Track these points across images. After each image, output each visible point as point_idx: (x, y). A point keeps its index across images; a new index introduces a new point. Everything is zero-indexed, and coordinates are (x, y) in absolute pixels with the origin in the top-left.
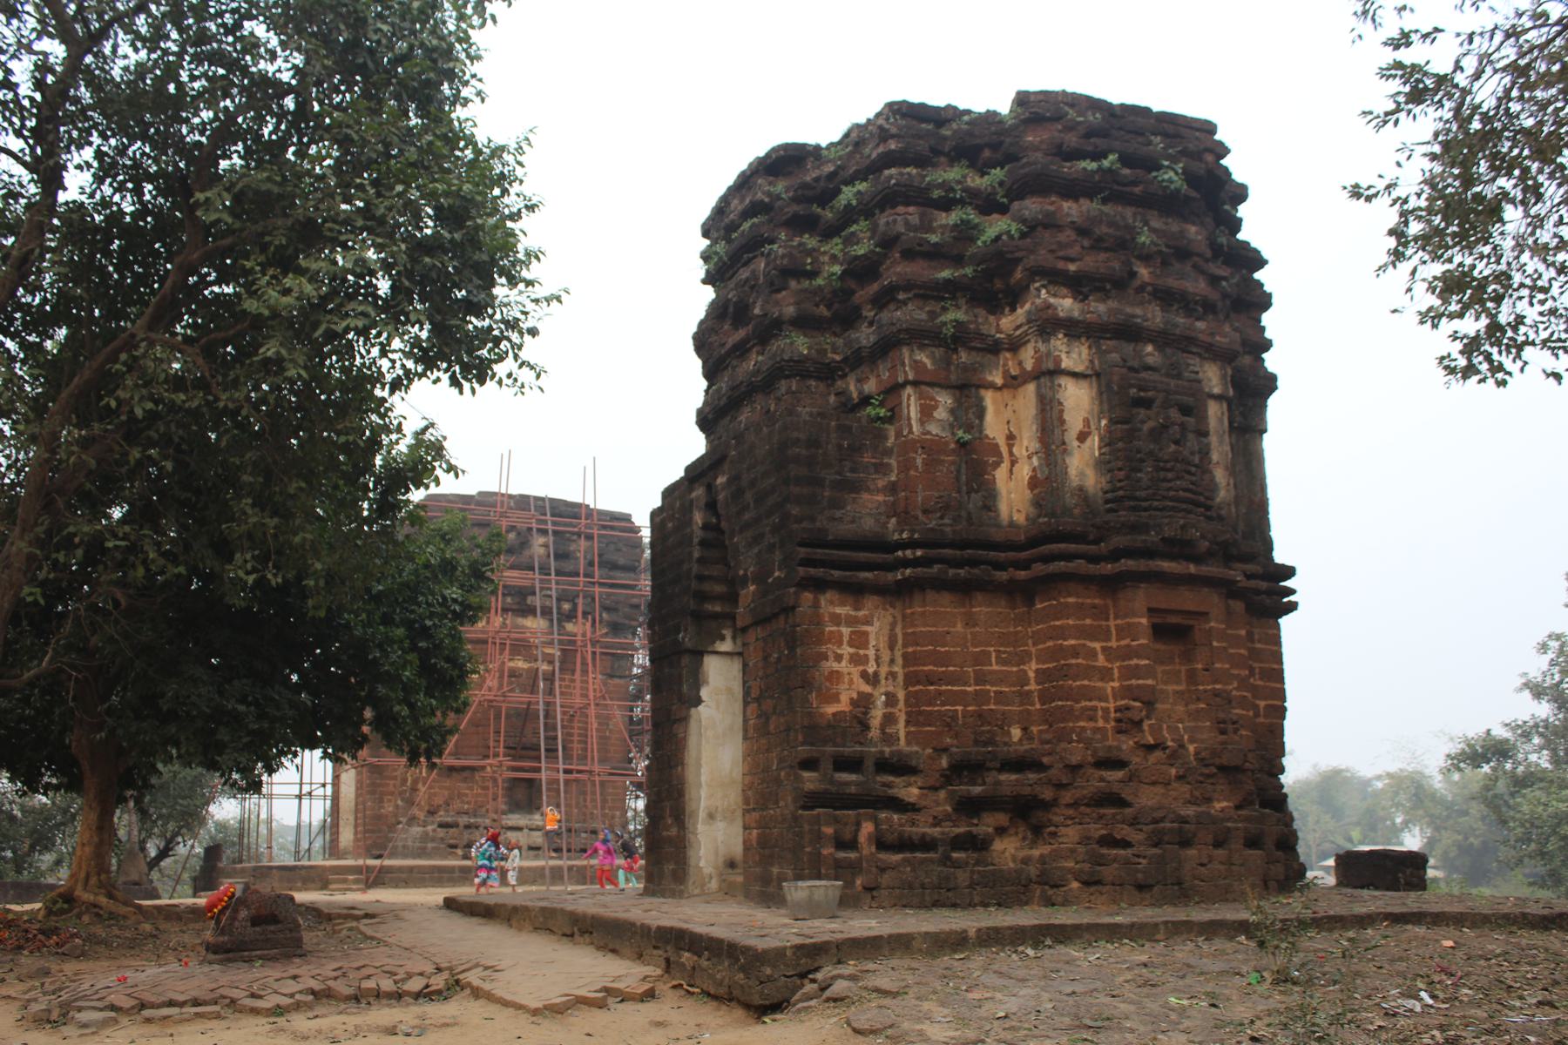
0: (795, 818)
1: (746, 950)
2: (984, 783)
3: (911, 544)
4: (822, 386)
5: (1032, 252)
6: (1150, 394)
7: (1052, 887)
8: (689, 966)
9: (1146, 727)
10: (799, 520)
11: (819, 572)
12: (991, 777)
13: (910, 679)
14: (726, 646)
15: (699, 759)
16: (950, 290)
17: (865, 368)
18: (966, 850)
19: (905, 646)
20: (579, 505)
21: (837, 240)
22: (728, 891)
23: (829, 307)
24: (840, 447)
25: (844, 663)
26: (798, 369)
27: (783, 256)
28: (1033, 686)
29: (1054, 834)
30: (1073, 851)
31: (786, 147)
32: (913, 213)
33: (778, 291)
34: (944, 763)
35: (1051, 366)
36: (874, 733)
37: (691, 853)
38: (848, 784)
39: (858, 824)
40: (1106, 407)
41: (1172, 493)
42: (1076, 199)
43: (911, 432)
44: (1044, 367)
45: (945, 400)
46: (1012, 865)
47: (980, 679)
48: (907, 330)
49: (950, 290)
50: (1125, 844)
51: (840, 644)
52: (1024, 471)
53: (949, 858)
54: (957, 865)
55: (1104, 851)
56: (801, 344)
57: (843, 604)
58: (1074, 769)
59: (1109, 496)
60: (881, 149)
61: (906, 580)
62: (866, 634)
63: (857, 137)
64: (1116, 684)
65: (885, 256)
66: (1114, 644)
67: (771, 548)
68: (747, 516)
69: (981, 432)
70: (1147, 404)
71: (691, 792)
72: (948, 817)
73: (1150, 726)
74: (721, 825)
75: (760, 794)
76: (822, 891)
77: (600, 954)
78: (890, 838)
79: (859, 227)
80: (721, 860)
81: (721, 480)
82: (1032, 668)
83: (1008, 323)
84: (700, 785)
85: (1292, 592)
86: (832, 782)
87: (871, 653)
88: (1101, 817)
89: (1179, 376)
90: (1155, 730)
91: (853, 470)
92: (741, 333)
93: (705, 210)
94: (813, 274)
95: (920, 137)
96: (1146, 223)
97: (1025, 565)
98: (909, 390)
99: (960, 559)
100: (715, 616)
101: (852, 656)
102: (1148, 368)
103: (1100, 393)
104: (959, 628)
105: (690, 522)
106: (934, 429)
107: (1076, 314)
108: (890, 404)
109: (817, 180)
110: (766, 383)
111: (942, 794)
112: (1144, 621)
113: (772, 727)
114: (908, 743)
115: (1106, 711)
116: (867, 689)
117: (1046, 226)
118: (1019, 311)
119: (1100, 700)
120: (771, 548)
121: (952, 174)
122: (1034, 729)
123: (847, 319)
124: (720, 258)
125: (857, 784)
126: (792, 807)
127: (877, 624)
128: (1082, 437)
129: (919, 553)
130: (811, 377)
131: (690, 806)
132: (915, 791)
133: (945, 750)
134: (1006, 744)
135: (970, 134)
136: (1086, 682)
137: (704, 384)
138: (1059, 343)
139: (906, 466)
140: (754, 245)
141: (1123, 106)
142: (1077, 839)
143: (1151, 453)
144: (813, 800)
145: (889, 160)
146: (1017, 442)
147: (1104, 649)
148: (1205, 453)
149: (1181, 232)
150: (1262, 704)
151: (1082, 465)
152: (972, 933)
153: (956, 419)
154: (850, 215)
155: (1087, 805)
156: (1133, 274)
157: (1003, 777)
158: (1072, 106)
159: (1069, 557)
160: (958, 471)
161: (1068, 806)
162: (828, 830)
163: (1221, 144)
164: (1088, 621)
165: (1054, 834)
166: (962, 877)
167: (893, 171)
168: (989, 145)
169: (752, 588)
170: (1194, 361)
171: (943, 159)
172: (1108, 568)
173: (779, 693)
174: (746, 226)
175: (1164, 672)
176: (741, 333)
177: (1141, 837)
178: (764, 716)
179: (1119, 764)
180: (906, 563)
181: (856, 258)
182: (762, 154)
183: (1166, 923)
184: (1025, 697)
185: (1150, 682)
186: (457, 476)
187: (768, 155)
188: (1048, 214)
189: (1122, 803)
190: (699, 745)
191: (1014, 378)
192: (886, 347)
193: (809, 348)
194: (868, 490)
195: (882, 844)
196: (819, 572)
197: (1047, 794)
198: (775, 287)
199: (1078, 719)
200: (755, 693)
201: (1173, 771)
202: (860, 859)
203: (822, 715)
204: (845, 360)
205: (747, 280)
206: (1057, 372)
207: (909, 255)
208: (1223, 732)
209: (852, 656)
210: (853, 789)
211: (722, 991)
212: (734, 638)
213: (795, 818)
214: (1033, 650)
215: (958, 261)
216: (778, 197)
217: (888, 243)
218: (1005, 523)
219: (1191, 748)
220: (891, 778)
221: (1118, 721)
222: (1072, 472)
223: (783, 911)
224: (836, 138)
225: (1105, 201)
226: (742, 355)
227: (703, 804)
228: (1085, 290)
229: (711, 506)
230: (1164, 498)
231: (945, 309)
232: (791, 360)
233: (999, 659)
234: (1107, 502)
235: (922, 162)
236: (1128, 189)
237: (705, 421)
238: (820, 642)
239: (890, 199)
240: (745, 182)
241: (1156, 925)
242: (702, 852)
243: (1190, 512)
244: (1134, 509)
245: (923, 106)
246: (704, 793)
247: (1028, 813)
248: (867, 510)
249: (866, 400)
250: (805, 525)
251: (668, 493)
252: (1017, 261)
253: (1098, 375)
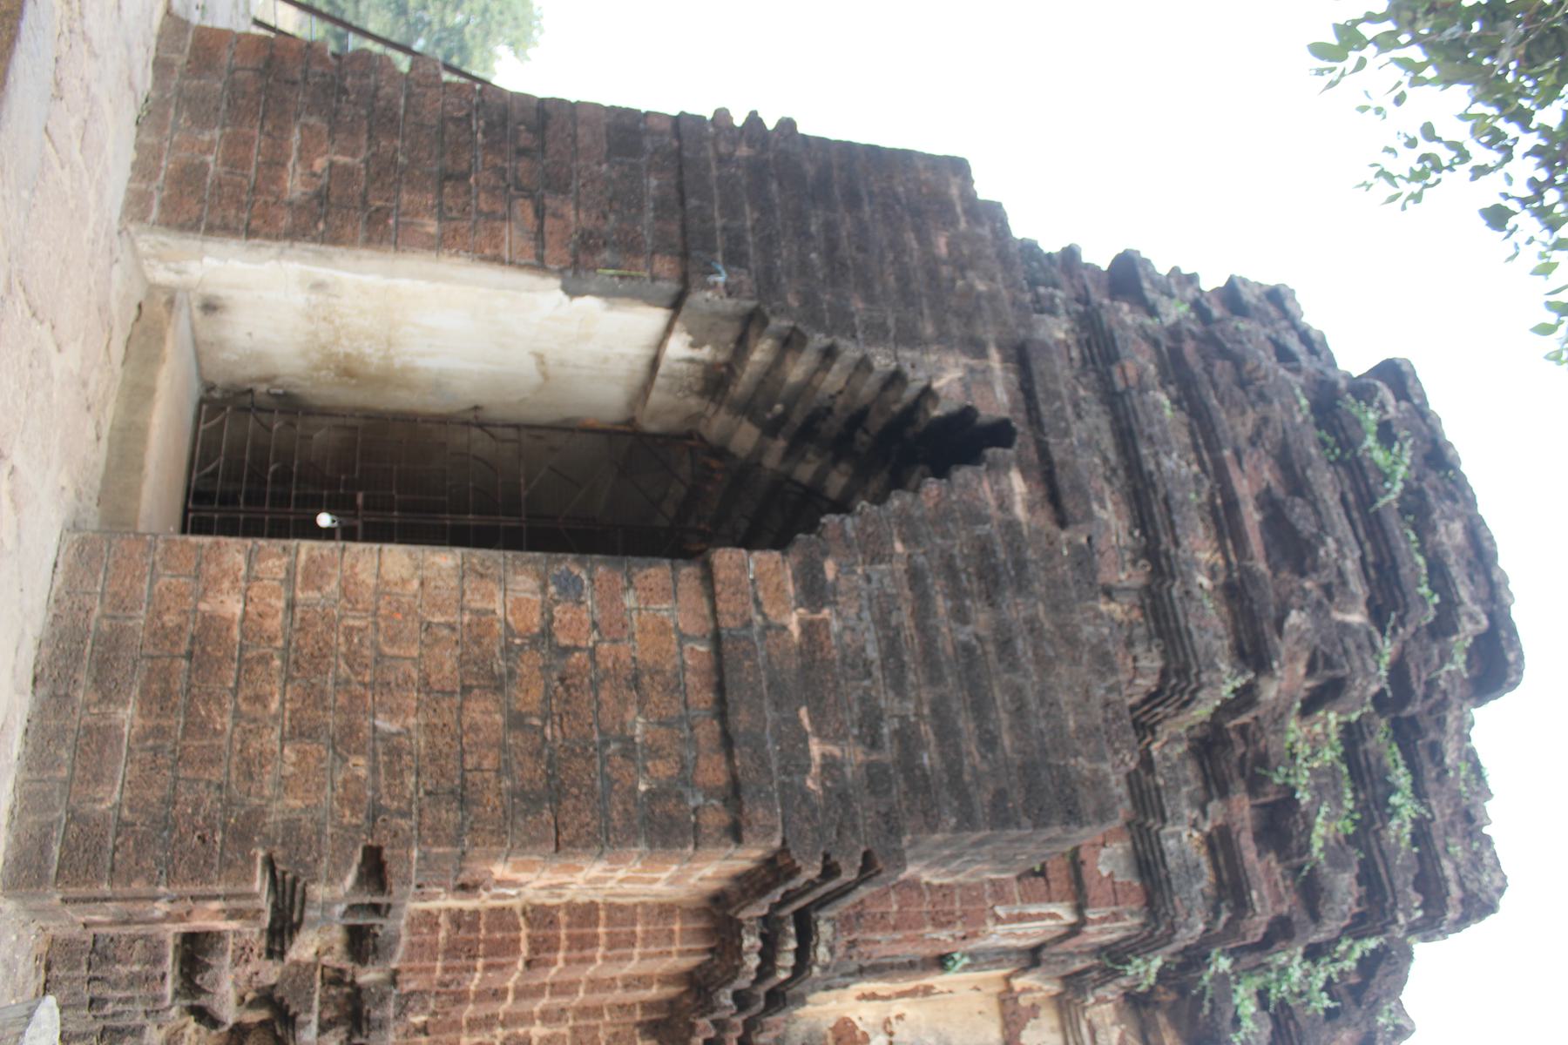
0: (242, 836)
14: (678, 347)
37: (234, 246)
43: (998, 920)
60: (1455, 891)
61: (738, 952)
74: (300, 298)
80: (222, 292)
100: (742, 344)
110: (1161, 616)
154: (1374, 809)
169: (793, 622)
186: (1319, 50)
212: (691, 361)
226: (1214, 510)
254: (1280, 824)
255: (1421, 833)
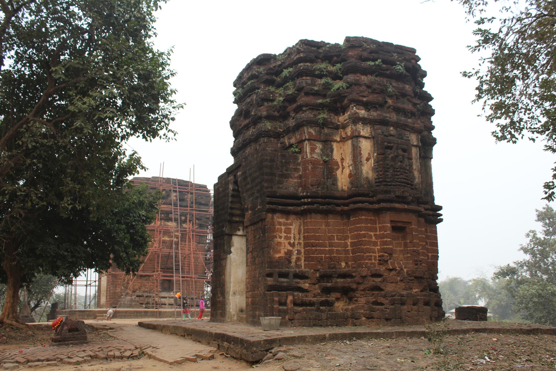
0: (265, 294)
1: (247, 341)
2: (332, 282)
3: (307, 197)
4: (275, 140)
5: (351, 94)
6: (392, 145)
7: (356, 319)
8: (226, 347)
9: (389, 263)
10: (267, 188)
11: (274, 207)
12: (334, 280)
13: (306, 245)
14: (240, 233)
15: (230, 273)
16: (321, 107)
17: (291, 134)
18: (325, 306)
19: (304, 233)
20: (188, 182)
21: (281, 88)
22: (240, 320)
23: (278, 112)
24: (282, 162)
25: (282, 239)
26: (267, 134)
27: (262, 94)
28: (349, 248)
29: (356, 301)
30: (363, 306)
31: (264, 55)
32: (309, 79)
33: (260, 106)
34: (318, 275)
35: (357, 134)
36: (293, 264)
37: (227, 307)
38: (283, 282)
39: (287, 297)
40: (376, 149)
41: (399, 180)
42: (366, 75)
43: (307, 157)
44: (354, 135)
45: (319, 146)
46: (341, 311)
47: (331, 245)
48: (306, 121)
49: (321, 107)
50: (382, 304)
51: (281, 232)
52: (347, 171)
53: (319, 309)
54: (322, 311)
55: (374, 306)
56: (268, 125)
57: (282, 218)
58: (364, 277)
59: (377, 180)
60: (297, 56)
61: (305, 210)
62: (290, 229)
63: (289, 52)
64: (379, 247)
65: (299, 94)
66: (378, 233)
67: (257, 198)
68: (248, 186)
69: (332, 157)
70: (390, 148)
71: (227, 285)
72: (319, 294)
73: (391, 262)
74: (238, 297)
75: (252, 285)
76: (274, 320)
77: (194, 343)
78: (298, 302)
79: (289, 84)
80: (238, 309)
81: (239, 173)
82: (349, 241)
83: (342, 119)
84: (230, 282)
85: (441, 215)
86: (278, 281)
87: (292, 235)
88: (373, 294)
89: (402, 138)
90: (392, 264)
91: (286, 170)
92: (247, 121)
93: (235, 78)
94: (273, 101)
95: (312, 52)
96: (391, 84)
97: (347, 205)
98: (306, 142)
99: (324, 202)
100: (237, 222)
101: (285, 236)
102: (391, 135)
103: (374, 144)
104: (324, 227)
105: (228, 188)
106: (315, 156)
107: (366, 116)
108: (300, 147)
109: (275, 67)
110: (256, 139)
111: (317, 286)
112: (389, 225)
113: (256, 262)
114: (305, 268)
115: (375, 257)
116: (291, 248)
117: (355, 85)
118: (346, 114)
119: (373, 253)
120: (257, 198)
121: (323, 66)
122: (350, 263)
123: (285, 117)
124: (240, 94)
125: (287, 282)
126: (263, 290)
127: (294, 225)
128: (368, 160)
129: (309, 200)
130: (271, 137)
131: (227, 290)
132: (307, 285)
133: (318, 270)
134: (339, 268)
135: (328, 51)
136: (368, 247)
137: (234, 139)
138: (360, 126)
139: (305, 169)
140: (252, 89)
141: (383, 42)
142: (364, 302)
143: (392, 166)
144: (271, 288)
145: (300, 60)
146: (345, 161)
147: (375, 235)
148: (411, 165)
149: (403, 87)
150: (430, 255)
151: (367, 169)
152: (327, 336)
153: (323, 153)
154: (286, 80)
155: (368, 290)
156: (386, 102)
157: (339, 280)
158: (365, 42)
159: (363, 202)
160: (324, 171)
161: (362, 290)
162: (276, 299)
163: (417, 56)
164: (369, 225)
165: (356, 301)
166: (324, 316)
167: (302, 64)
168: (335, 56)
169: (250, 212)
170: (407, 133)
171: (319, 60)
172: (376, 206)
173: (259, 251)
174: (249, 83)
175: (396, 243)
176: (247, 121)
177: (387, 301)
178: (254, 258)
179: (380, 276)
180: (305, 204)
181: (288, 95)
182: (255, 57)
183: (396, 332)
184: (347, 252)
185: (391, 247)
186: (145, 170)
187: (257, 58)
188: (357, 80)
189: (380, 289)
190: (231, 268)
191: (344, 138)
192: (298, 127)
193: (271, 127)
194: (292, 177)
195: (295, 304)
196: (274, 207)
197: (354, 286)
198: (259, 105)
199: (365, 259)
200: (250, 250)
201: (399, 278)
202: (288, 309)
203: (274, 257)
204: (284, 131)
205: (249, 102)
206: (359, 136)
207: (307, 94)
208: (416, 265)
209: (285, 236)
210: (285, 284)
211: (238, 356)
212: (243, 230)
213: (265, 294)
214: (350, 235)
215: (324, 96)
216: (261, 73)
217: (300, 90)
218: (340, 190)
219: (405, 270)
220: (299, 280)
221: (380, 260)
222: (364, 172)
223: (260, 328)
224: (282, 52)
225: (376, 76)
226: (247, 129)
227: (231, 289)
228: (369, 107)
229: (236, 183)
230: (397, 181)
231: (319, 114)
232: (264, 131)
233: (338, 238)
234: (376, 183)
235: (312, 61)
236: (385, 72)
237: (234, 152)
238: (274, 231)
239: (300, 74)
240: (249, 67)
241: (392, 333)
242: (231, 306)
243: (406, 186)
244: (386, 185)
245: (313, 41)
246: (232, 285)
247: (347, 293)
248: (291, 185)
249: (291, 146)
250: (269, 190)
251: (220, 178)
252: (345, 97)
253: (373, 138)
254: (290, 99)
255: (290, 66)
